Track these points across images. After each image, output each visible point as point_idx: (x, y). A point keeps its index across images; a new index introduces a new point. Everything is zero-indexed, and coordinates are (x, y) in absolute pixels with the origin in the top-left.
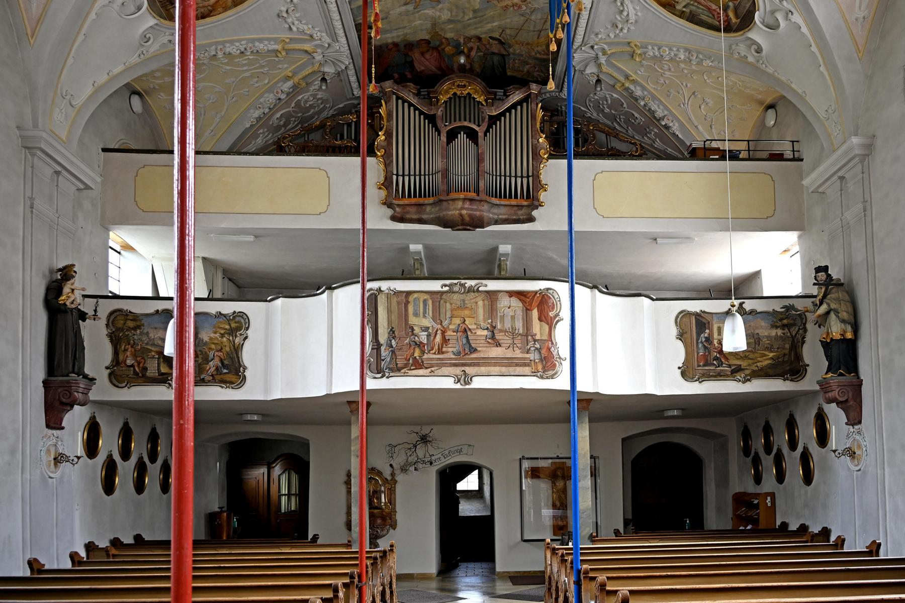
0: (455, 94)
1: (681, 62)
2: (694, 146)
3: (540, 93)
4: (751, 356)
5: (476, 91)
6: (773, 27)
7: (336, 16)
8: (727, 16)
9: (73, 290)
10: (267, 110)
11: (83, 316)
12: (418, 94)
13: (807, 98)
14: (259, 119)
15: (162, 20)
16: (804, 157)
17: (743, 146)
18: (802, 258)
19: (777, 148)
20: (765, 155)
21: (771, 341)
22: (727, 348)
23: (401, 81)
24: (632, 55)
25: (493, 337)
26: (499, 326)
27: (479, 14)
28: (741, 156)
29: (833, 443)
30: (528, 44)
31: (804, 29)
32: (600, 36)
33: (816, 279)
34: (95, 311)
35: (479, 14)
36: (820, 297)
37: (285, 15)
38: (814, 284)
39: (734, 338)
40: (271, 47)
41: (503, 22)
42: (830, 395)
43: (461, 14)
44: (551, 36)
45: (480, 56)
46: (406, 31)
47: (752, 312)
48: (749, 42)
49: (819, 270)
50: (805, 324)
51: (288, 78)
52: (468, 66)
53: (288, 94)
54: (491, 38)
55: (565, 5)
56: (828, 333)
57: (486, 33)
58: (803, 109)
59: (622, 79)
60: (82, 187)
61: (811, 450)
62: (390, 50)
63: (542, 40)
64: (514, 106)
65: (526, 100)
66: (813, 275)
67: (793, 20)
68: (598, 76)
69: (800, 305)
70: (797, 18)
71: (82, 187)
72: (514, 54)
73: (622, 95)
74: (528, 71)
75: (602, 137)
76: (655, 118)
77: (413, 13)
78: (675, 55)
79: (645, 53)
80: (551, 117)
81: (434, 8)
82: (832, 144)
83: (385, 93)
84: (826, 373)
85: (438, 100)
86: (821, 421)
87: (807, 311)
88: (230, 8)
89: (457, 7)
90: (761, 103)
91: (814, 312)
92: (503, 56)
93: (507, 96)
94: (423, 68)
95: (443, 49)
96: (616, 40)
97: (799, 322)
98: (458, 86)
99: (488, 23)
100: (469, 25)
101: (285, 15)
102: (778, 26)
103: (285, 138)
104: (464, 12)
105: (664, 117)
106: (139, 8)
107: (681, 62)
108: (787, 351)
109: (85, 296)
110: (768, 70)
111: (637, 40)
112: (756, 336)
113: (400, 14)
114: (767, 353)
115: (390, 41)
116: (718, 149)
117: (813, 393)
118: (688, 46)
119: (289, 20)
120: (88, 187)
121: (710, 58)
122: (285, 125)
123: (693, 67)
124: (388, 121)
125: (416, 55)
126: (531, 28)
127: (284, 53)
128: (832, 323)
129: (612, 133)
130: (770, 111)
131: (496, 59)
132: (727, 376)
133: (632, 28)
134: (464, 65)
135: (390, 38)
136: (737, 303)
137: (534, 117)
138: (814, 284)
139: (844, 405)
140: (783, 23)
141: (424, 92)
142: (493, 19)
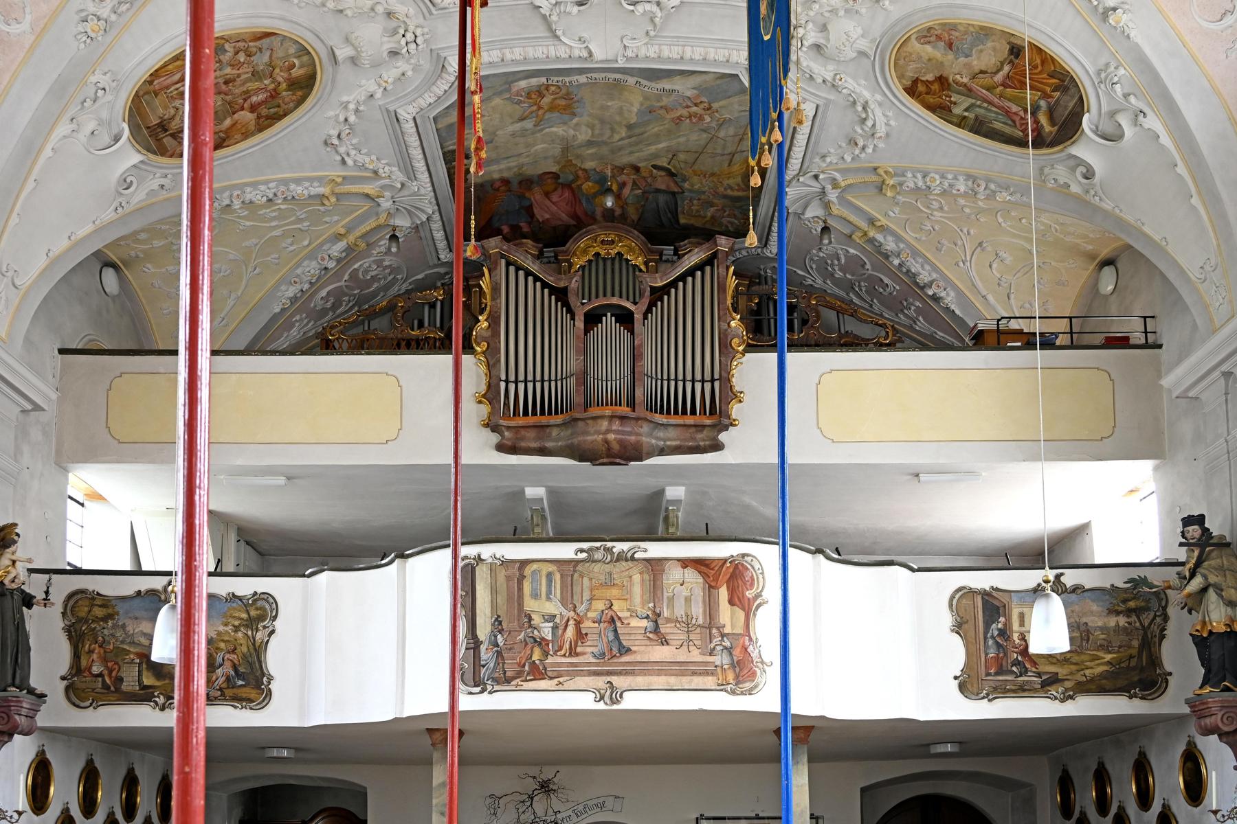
0: (597, 255)
1: (961, 196)
2: (980, 327)
3: (732, 250)
4: (1075, 659)
5: (631, 250)
6: (1113, 137)
7: (413, 141)
8: (1036, 122)
9: (14, 562)
10: (306, 286)
11: (28, 601)
12: (539, 256)
13: (1170, 249)
14: (294, 300)
15: (151, 156)
16: (1164, 342)
17: (1062, 325)
18: (1160, 502)
19: (1118, 328)
20: (1099, 339)
21: (1108, 634)
22: (1037, 646)
23: (514, 236)
24: (880, 188)
27: (637, 131)
28: (1058, 342)
29: (1213, 797)
30: (713, 174)
31: (1165, 140)
32: (828, 160)
33: (1183, 536)
34: (47, 593)
35: (637, 131)
36: (1191, 565)
37: (336, 142)
38: (1181, 545)
39: (1048, 630)
40: (314, 191)
41: (674, 142)
42: (1208, 721)
43: (608, 133)
44: (752, 163)
45: (637, 196)
46: (523, 160)
47: (1076, 589)
48: (1072, 162)
49: (1188, 521)
50: (1165, 608)
51: (338, 237)
52: (618, 212)
53: (339, 261)
54: (655, 167)
55: (775, 115)
56: (1204, 623)
57: (646, 160)
58: (1162, 266)
59: (863, 225)
60: (29, 407)
61: (1174, 809)
62: (498, 190)
63: (736, 168)
64: (691, 272)
65: (710, 261)
66: (1180, 529)
67: (1146, 126)
68: (825, 222)
69: (1156, 577)
70: (1152, 122)
71: (29, 407)
72: (690, 191)
73: (863, 250)
74: (713, 217)
75: (830, 315)
76: (917, 284)
77: (533, 133)
78: (951, 186)
79: (901, 184)
80: (749, 286)
81: (565, 123)
82: (1212, 320)
83: (486, 254)
84: (1201, 688)
85: (571, 265)
86: (1192, 764)
87: (1169, 587)
88: (253, 134)
89: (602, 122)
90: (1092, 257)
91: (1181, 589)
92: (674, 194)
93: (680, 257)
94: (547, 216)
95: (579, 187)
96: (852, 166)
97: (1154, 604)
98: (603, 242)
99: (650, 145)
100: (620, 149)
101: (336, 142)
102: (1122, 136)
103: (333, 327)
104: (613, 130)
105: (931, 283)
106: (117, 139)
107: (961, 196)
108: (1134, 652)
109: (31, 571)
110: (1104, 205)
111: (888, 163)
112: (1083, 628)
113: (513, 135)
114: (1101, 654)
115: (496, 176)
116: (1020, 332)
117: (1180, 719)
118: (973, 172)
119: (342, 150)
120: (37, 408)
121: (1007, 188)
122: (334, 307)
123: (980, 203)
124: (493, 299)
125: (536, 196)
126: (719, 151)
127: (333, 200)
128: (1212, 607)
129: (845, 309)
130: (1106, 268)
131: (662, 199)
132: (1035, 690)
133: (881, 145)
134: (611, 210)
135: (496, 171)
136: (1051, 574)
137: (723, 288)
138: (1181, 545)
139: (1231, 738)
140: (1129, 131)
141: (549, 252)
142: (657, 138)
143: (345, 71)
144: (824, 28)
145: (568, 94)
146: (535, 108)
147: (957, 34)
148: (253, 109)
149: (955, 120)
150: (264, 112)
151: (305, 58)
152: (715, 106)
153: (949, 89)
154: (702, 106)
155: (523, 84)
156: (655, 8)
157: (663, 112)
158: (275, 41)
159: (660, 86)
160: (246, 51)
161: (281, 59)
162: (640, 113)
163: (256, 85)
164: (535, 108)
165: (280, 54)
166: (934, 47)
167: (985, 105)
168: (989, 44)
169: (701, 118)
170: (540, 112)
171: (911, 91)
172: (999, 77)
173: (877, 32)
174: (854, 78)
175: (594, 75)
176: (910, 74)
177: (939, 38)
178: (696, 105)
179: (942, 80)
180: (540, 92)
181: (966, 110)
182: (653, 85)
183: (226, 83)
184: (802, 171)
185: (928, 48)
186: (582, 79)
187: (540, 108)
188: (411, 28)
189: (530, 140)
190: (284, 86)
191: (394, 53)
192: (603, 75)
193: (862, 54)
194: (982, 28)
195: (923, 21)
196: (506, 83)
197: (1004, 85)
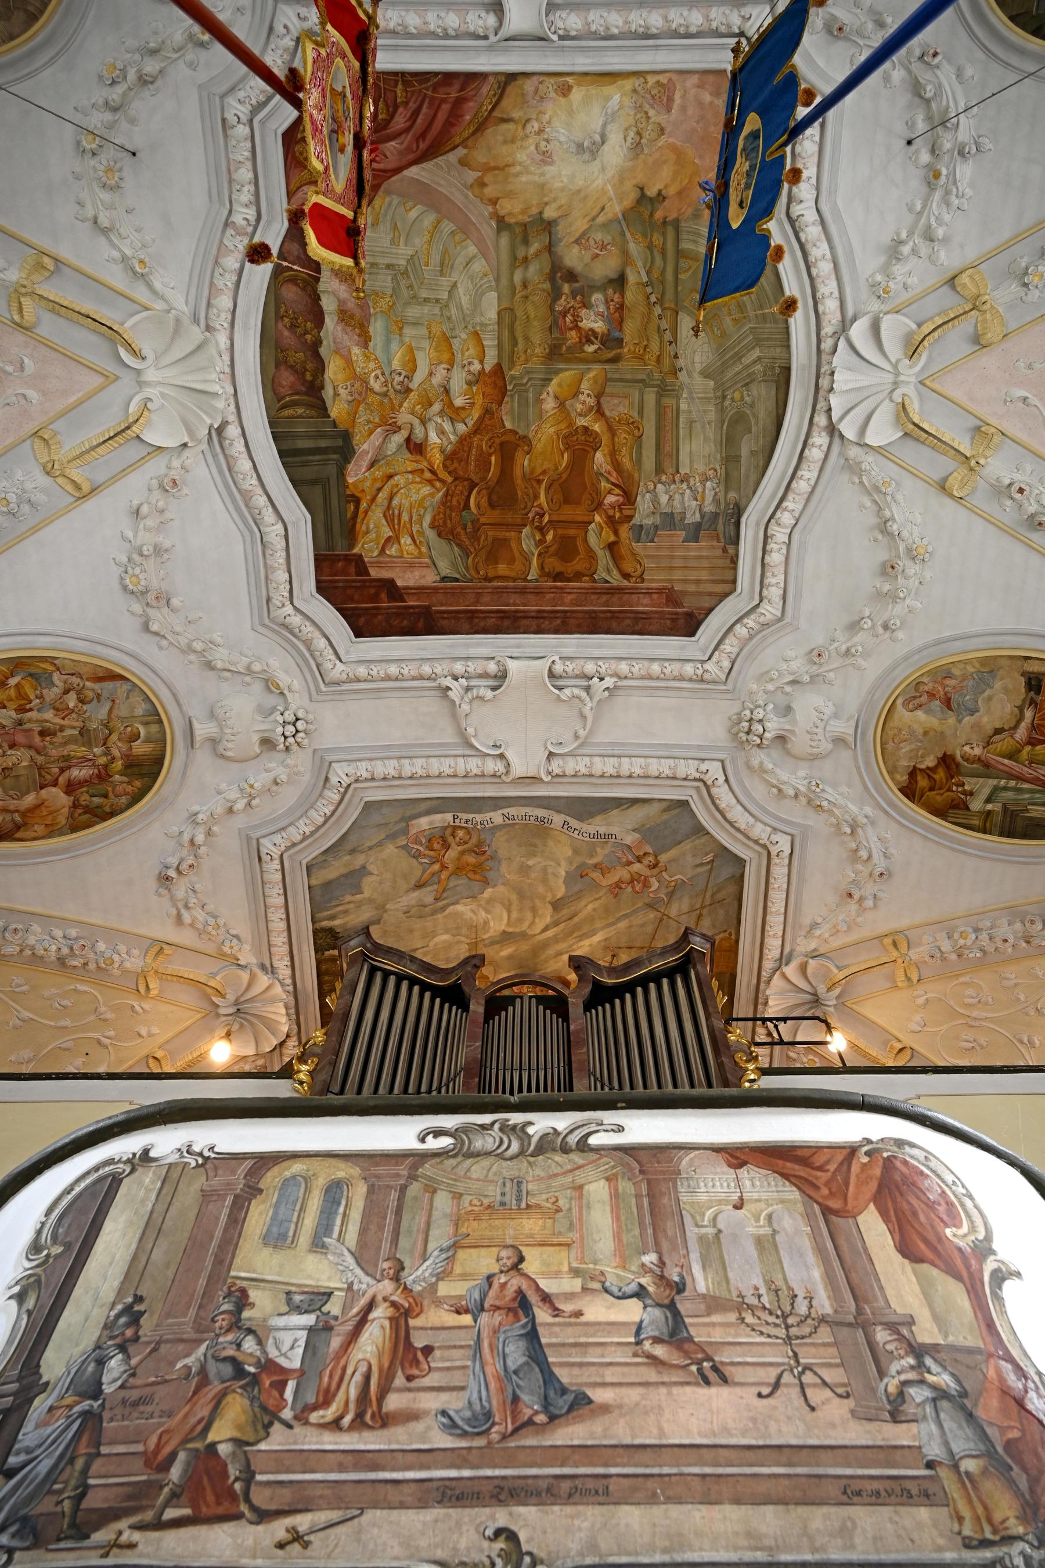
25: (676, 1332)
26: (701, 1281)
27: (565, 912)
43: (529, 915)
77: (434, 912)
88: (61, 833)
100: (546, 945)
143: (202, 757)
144: (787, 710)
145: (480, 844)
146: (436, 867)
147: (952, 682)
148: (70, 788)
149: (976, 822)
150: (85, 799)
151: (154, 728)
152: (663, 858)
153: (959, 774)
154: (646, 861)
155: (424, 823)
156: (583, 694)
157: (596, 875)
158: (122, 688)
159: (592, 829)
160: (79, 693)
161: (122, 719)
162: (569, 879)
163: (81, 751)
164: (436, 867)
165: (123, 711)
166: (927, 712)
167: (1012, 783)
168: (998, 685)
169: (646, 885)
170: (444, 875)
171: (909, 791)
172: (1021, 733)
173: (852, 705)
174: (835, 785)
175: (512, 811)
176: (905, 763)
177: (931, 695)
178: (639, 860)
179: (946, 761)
180: (442, 839)
181: (988, 800)
182: (584, 827)
183: (42, 733)
184: (784, 959)
185: (920, 714)
186: (497, 817)
187: (444, 867)
188: (293, 707)
189: (428, 923)
190: (118, 765)
191: (267, 743)
192: (523, 810)
193: (839, 741)
194: (984, 661)
195: (906, 674)
196: (402, 819)
197: (1032, 742)
